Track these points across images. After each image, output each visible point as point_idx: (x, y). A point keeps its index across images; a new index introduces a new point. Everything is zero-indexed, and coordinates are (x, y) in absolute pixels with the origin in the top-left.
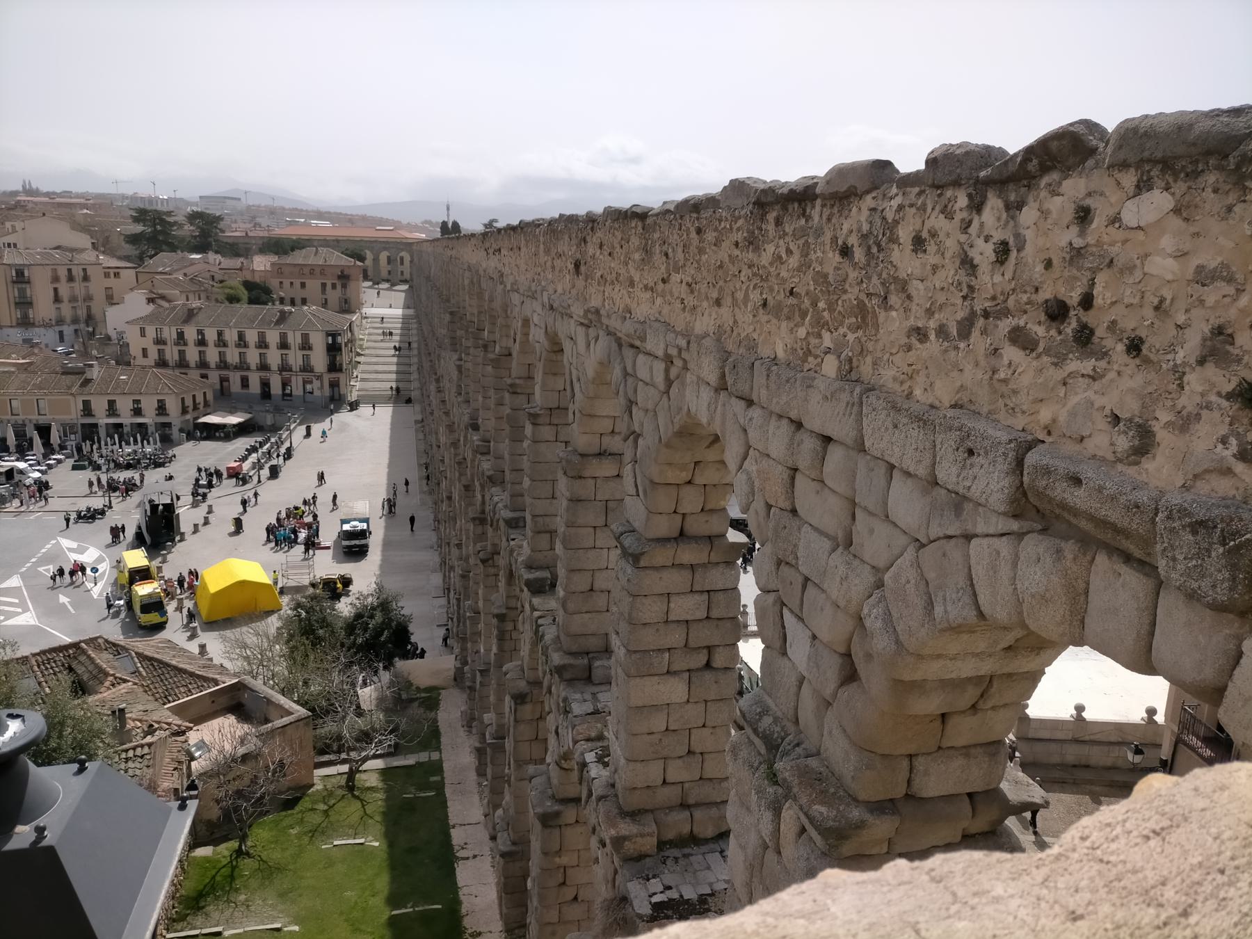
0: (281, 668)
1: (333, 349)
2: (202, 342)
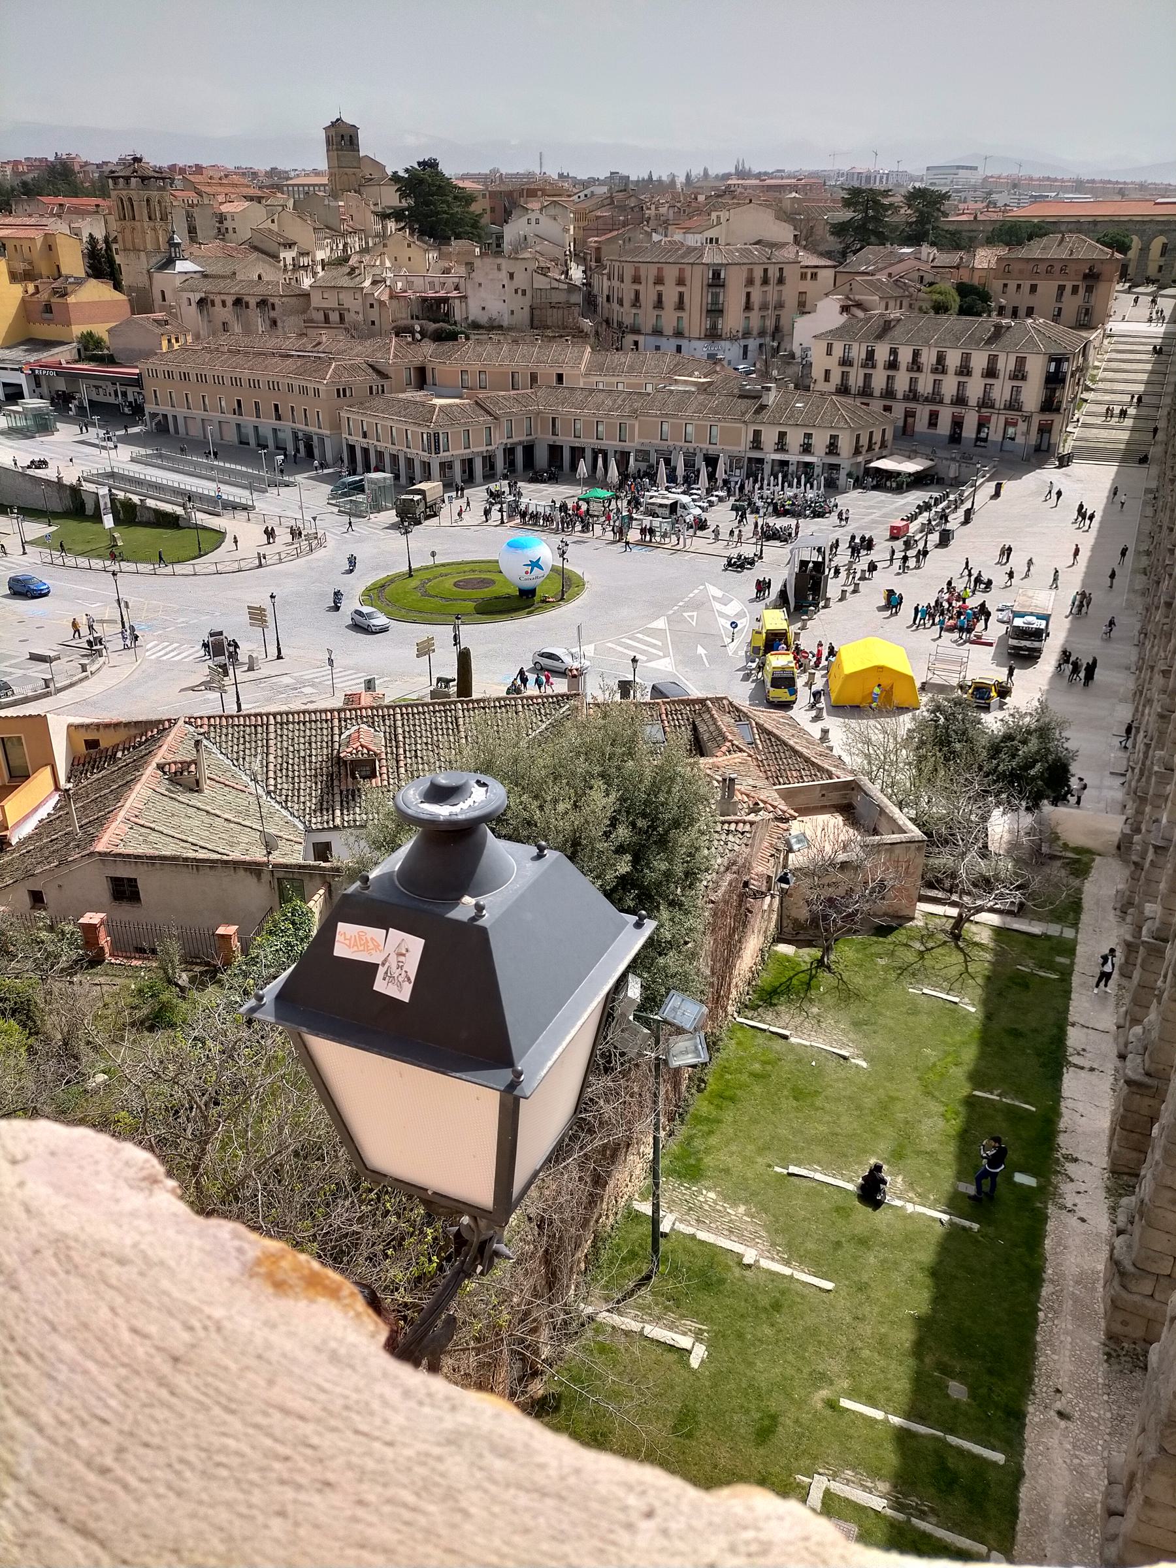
0: (904, 778)
1: (1054, 380)
2: (893, 365)
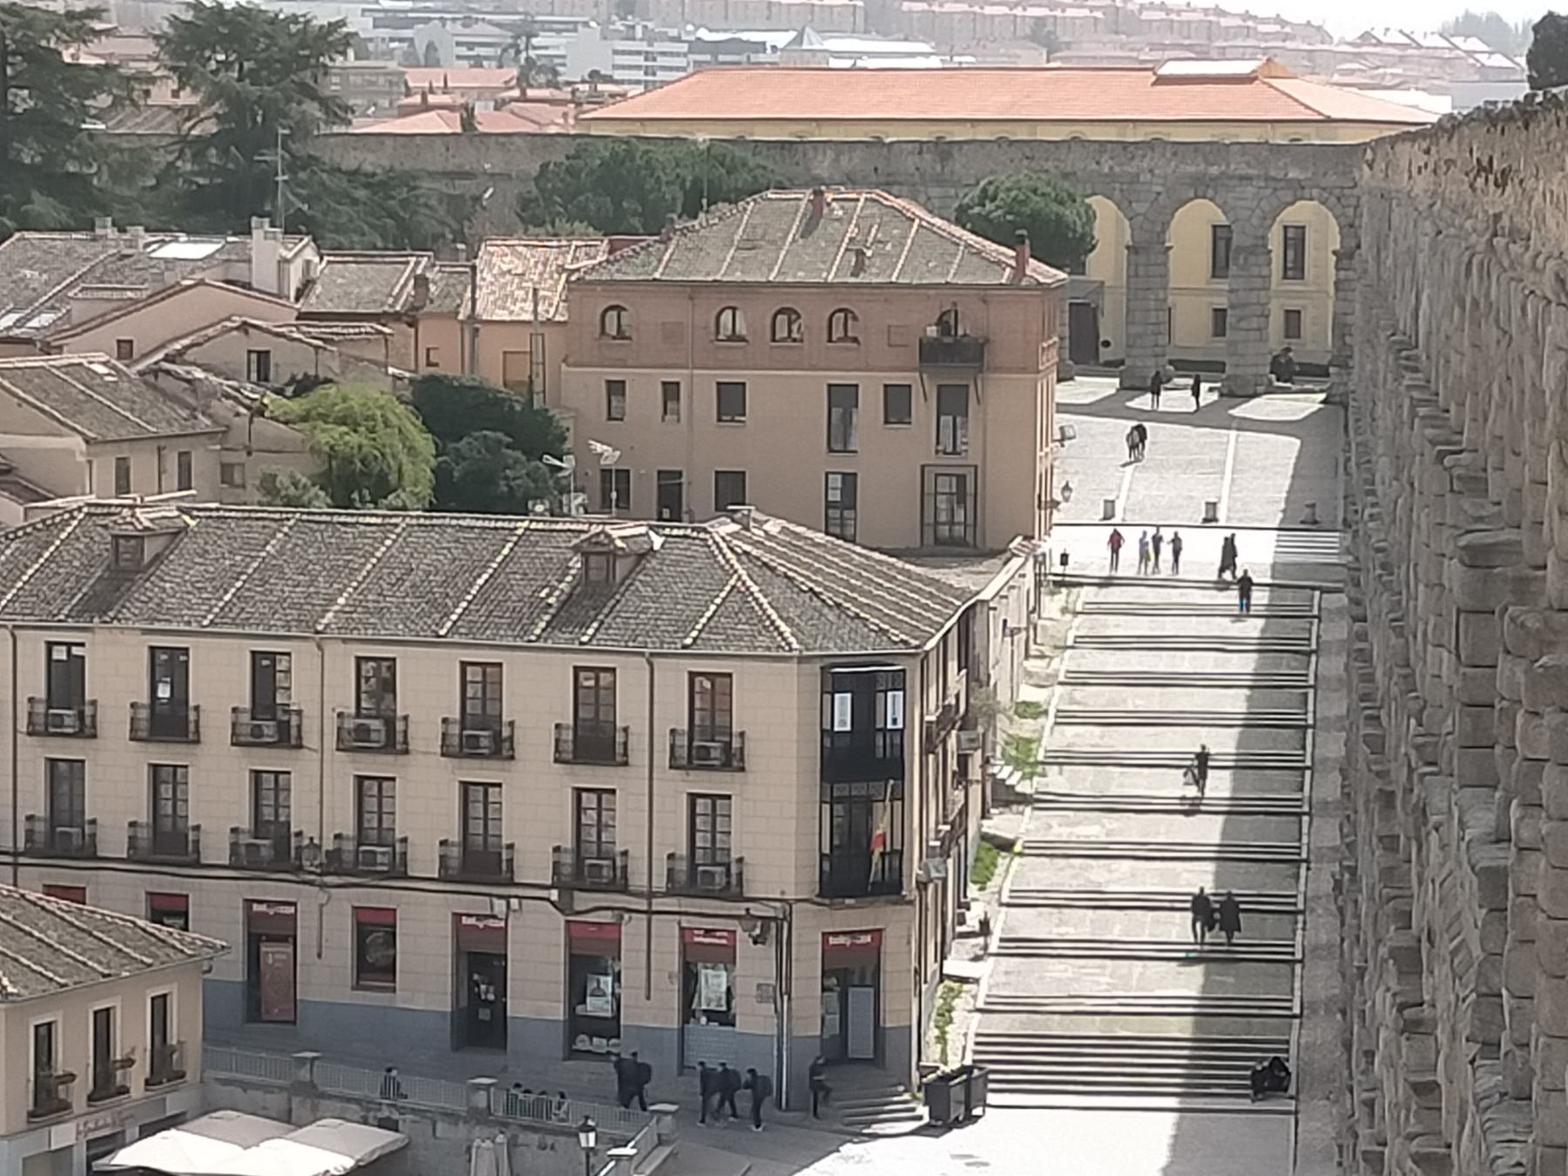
1: (858, 766)
2: (169, 721)
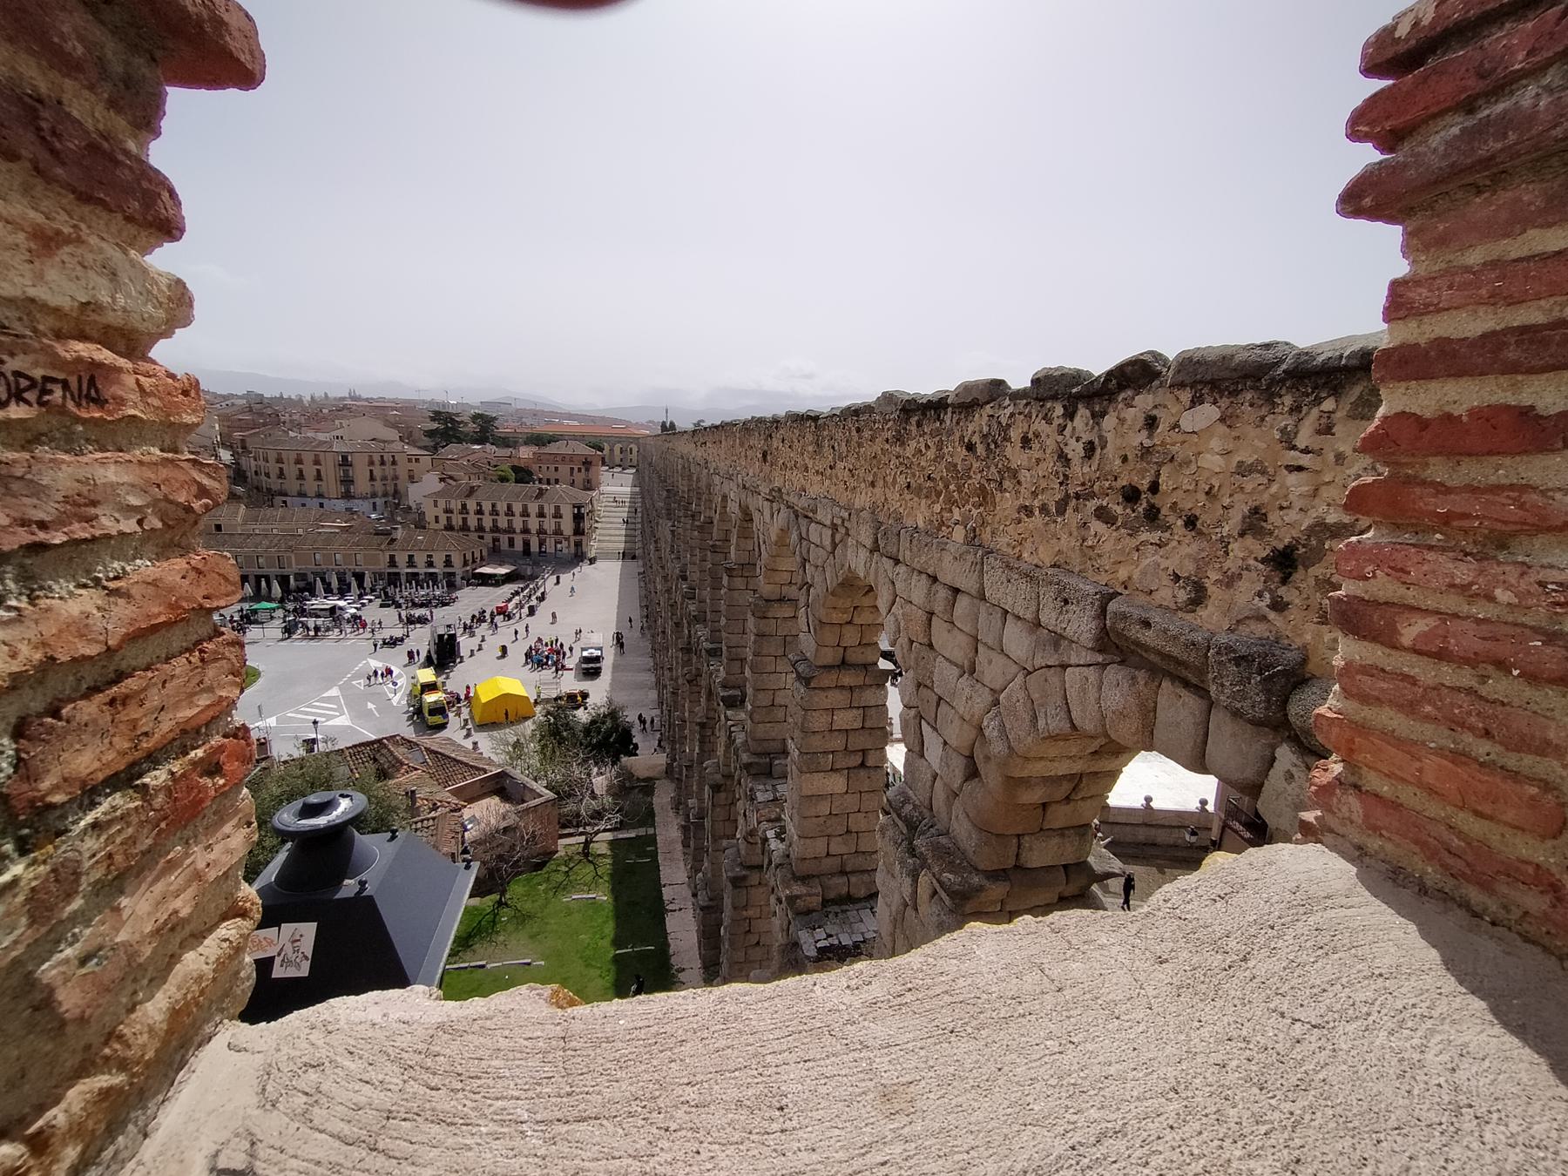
0: (535, 761)
2: (480, 512)
